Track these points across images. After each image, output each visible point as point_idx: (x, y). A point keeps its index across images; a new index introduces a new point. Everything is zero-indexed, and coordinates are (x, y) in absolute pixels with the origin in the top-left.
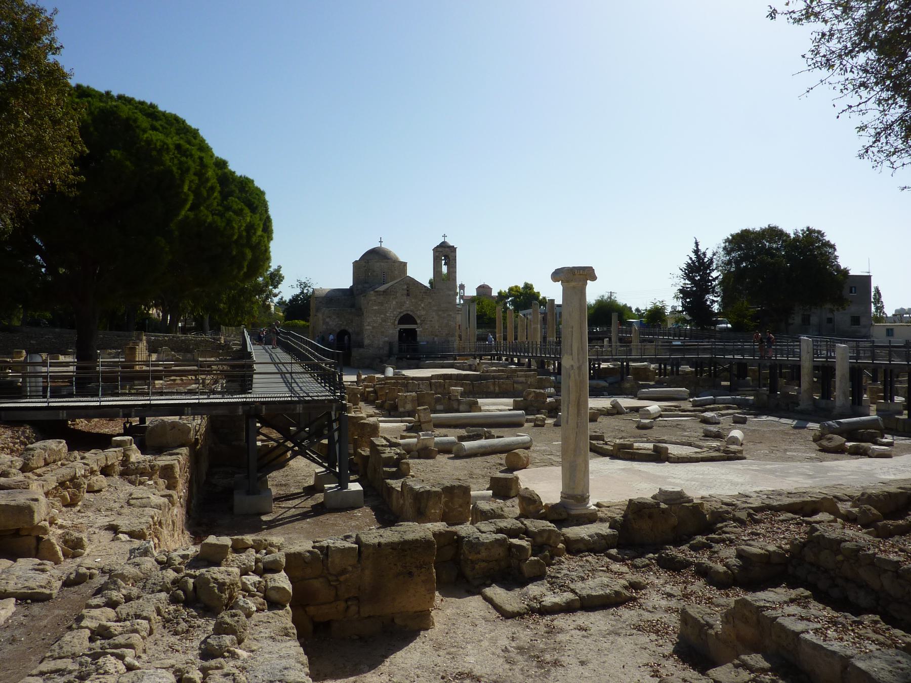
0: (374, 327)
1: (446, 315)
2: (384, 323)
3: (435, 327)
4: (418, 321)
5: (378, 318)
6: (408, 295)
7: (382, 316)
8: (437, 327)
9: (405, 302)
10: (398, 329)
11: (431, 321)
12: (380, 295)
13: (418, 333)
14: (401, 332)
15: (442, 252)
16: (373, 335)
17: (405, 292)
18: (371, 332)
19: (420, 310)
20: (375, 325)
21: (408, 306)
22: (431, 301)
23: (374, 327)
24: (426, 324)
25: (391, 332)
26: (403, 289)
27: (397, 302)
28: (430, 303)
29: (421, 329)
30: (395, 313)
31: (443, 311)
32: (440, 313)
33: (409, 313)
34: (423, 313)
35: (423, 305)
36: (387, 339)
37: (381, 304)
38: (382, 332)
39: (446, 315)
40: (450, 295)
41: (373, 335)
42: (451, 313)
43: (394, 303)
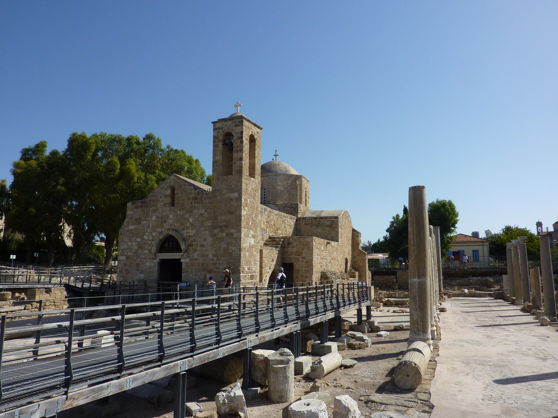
0: (128, 258)
1: (224, 234)
2: (140, 251)
3: (208, 256)
4: (183, 247)
5: (133, 243)
6: (173, 204)
7: (139, 240)
8: (210, 256)
9: (168, 217)
10: (157, 260)
11: (203, 246)
12: (137, 207)
13: (184, 266)
14: (163, 263)
15: (222, 128)
16: (126, 270)
17: (169, 200)
18: (125, 265)
19: (188, 228)
20: (129, 254)
21: (170, 221)
22: (203, 211)
23: (128, 258)
24: (195, 251)
25: (148, 264)
26: (166, 196)
27: (157, 217)
28: (201, 215)
29: (187, 260)
30: (154, 234)
31: (220, 227)
32: (216, 231)
33: (171, 233)
34: (192, 232)
35: (191, 220)
36: (142, 276)
37: (138, 221)
38: (138, 265)
39: (224, 234)
40: (231, 199)
41: (126, 270)
42: (232, 231)
43: (154, 218)
